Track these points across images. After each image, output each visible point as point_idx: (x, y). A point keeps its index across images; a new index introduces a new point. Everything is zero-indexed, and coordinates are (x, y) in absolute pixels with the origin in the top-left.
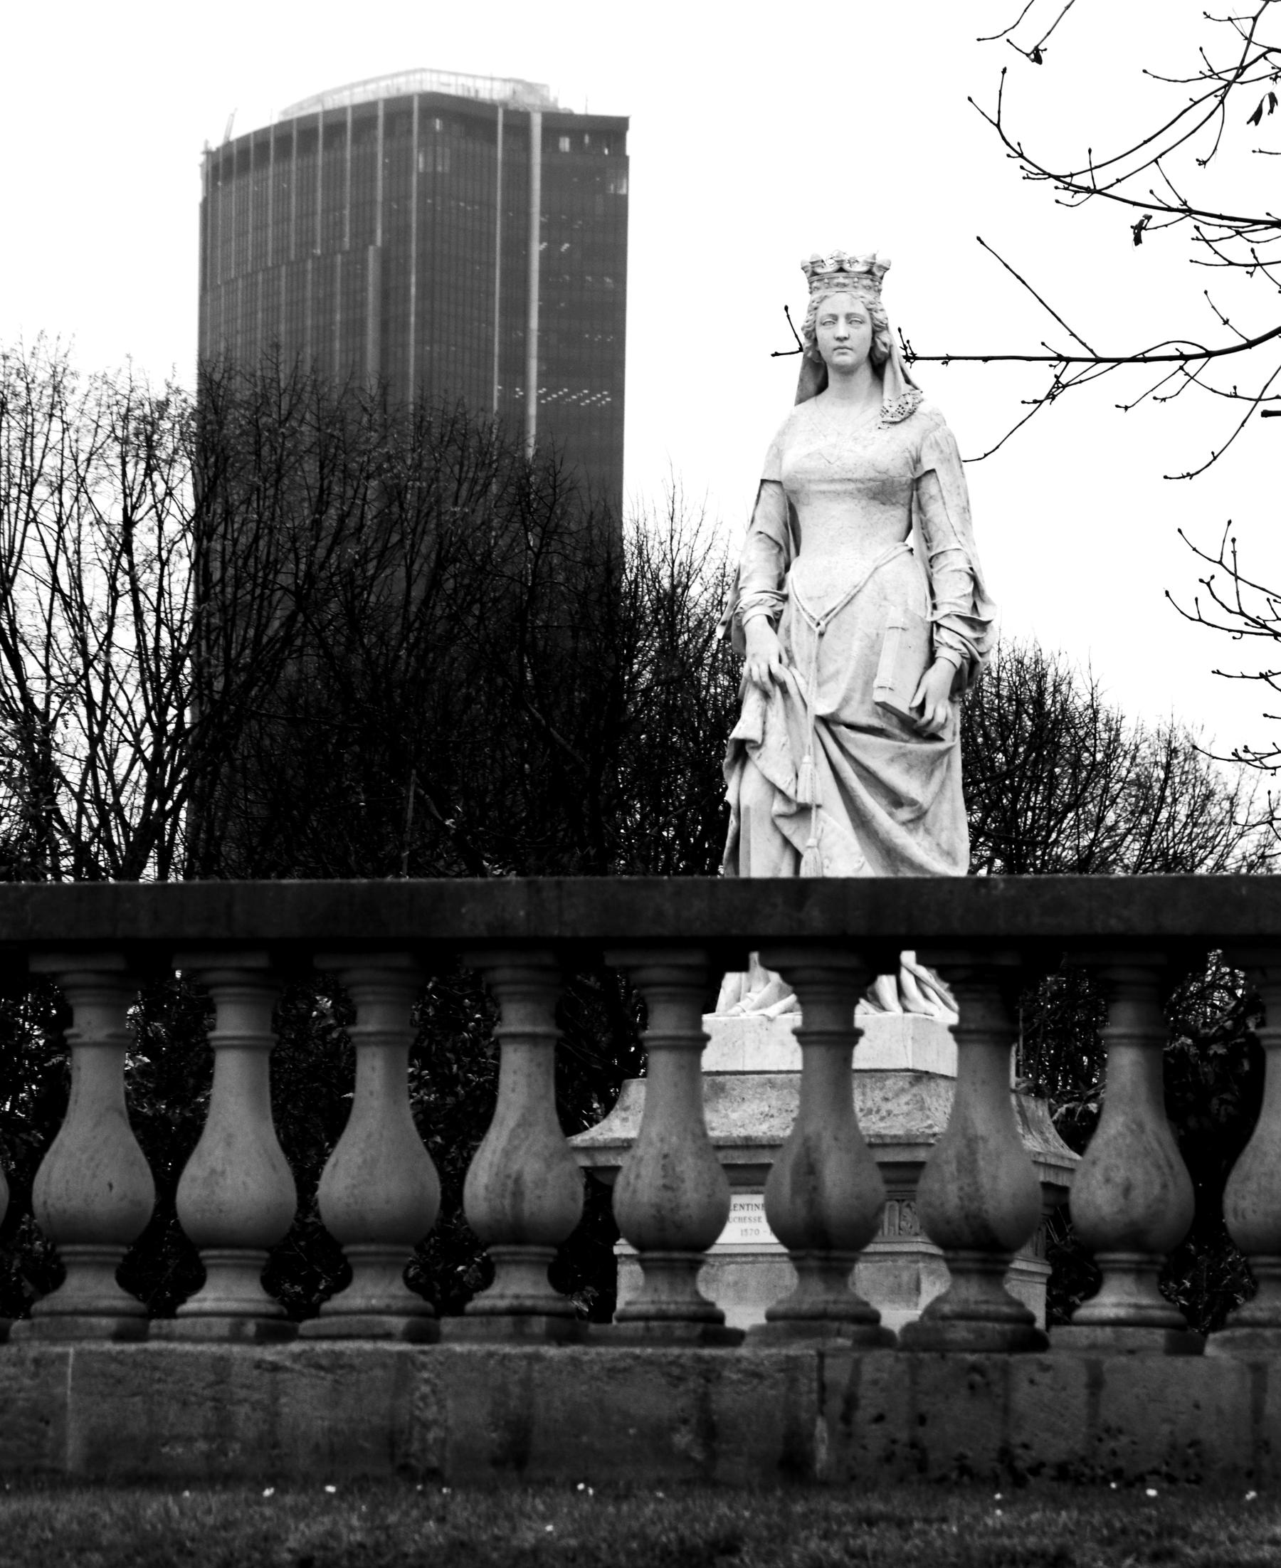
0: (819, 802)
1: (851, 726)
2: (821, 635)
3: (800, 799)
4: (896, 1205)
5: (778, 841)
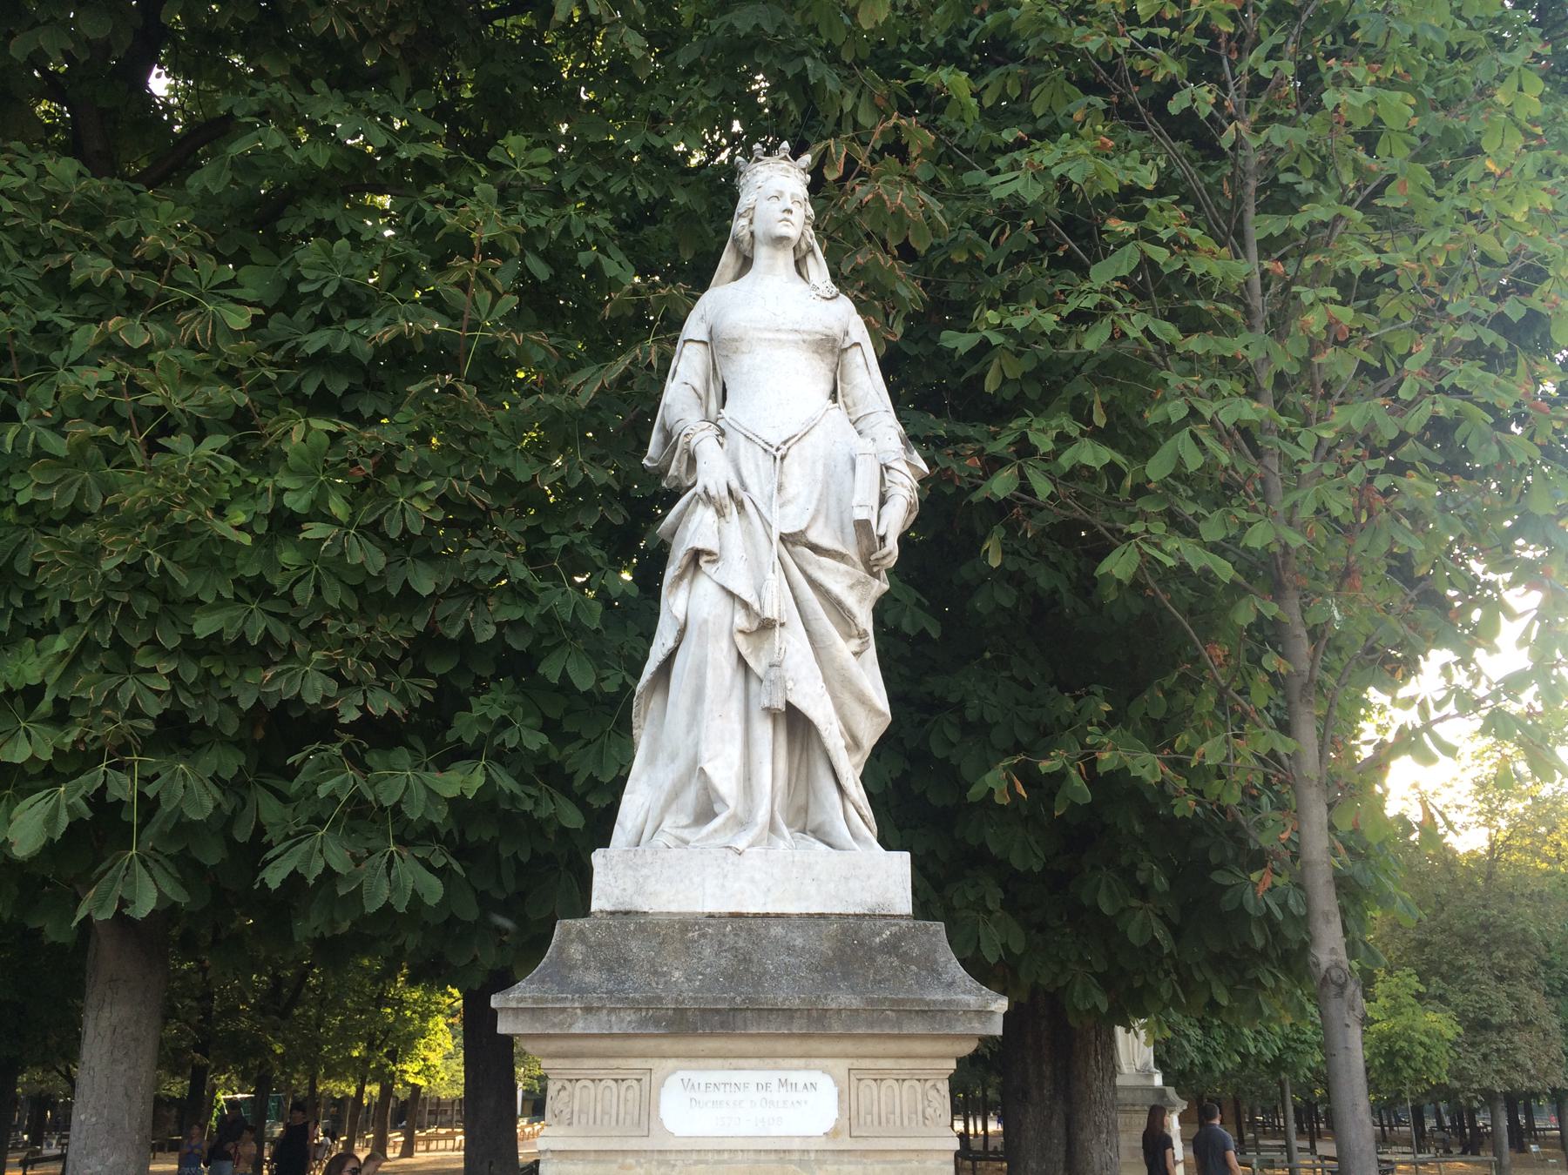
1: (815, 549)
2: (783, 458)
3: (768, 614)
4: (896, 1085)
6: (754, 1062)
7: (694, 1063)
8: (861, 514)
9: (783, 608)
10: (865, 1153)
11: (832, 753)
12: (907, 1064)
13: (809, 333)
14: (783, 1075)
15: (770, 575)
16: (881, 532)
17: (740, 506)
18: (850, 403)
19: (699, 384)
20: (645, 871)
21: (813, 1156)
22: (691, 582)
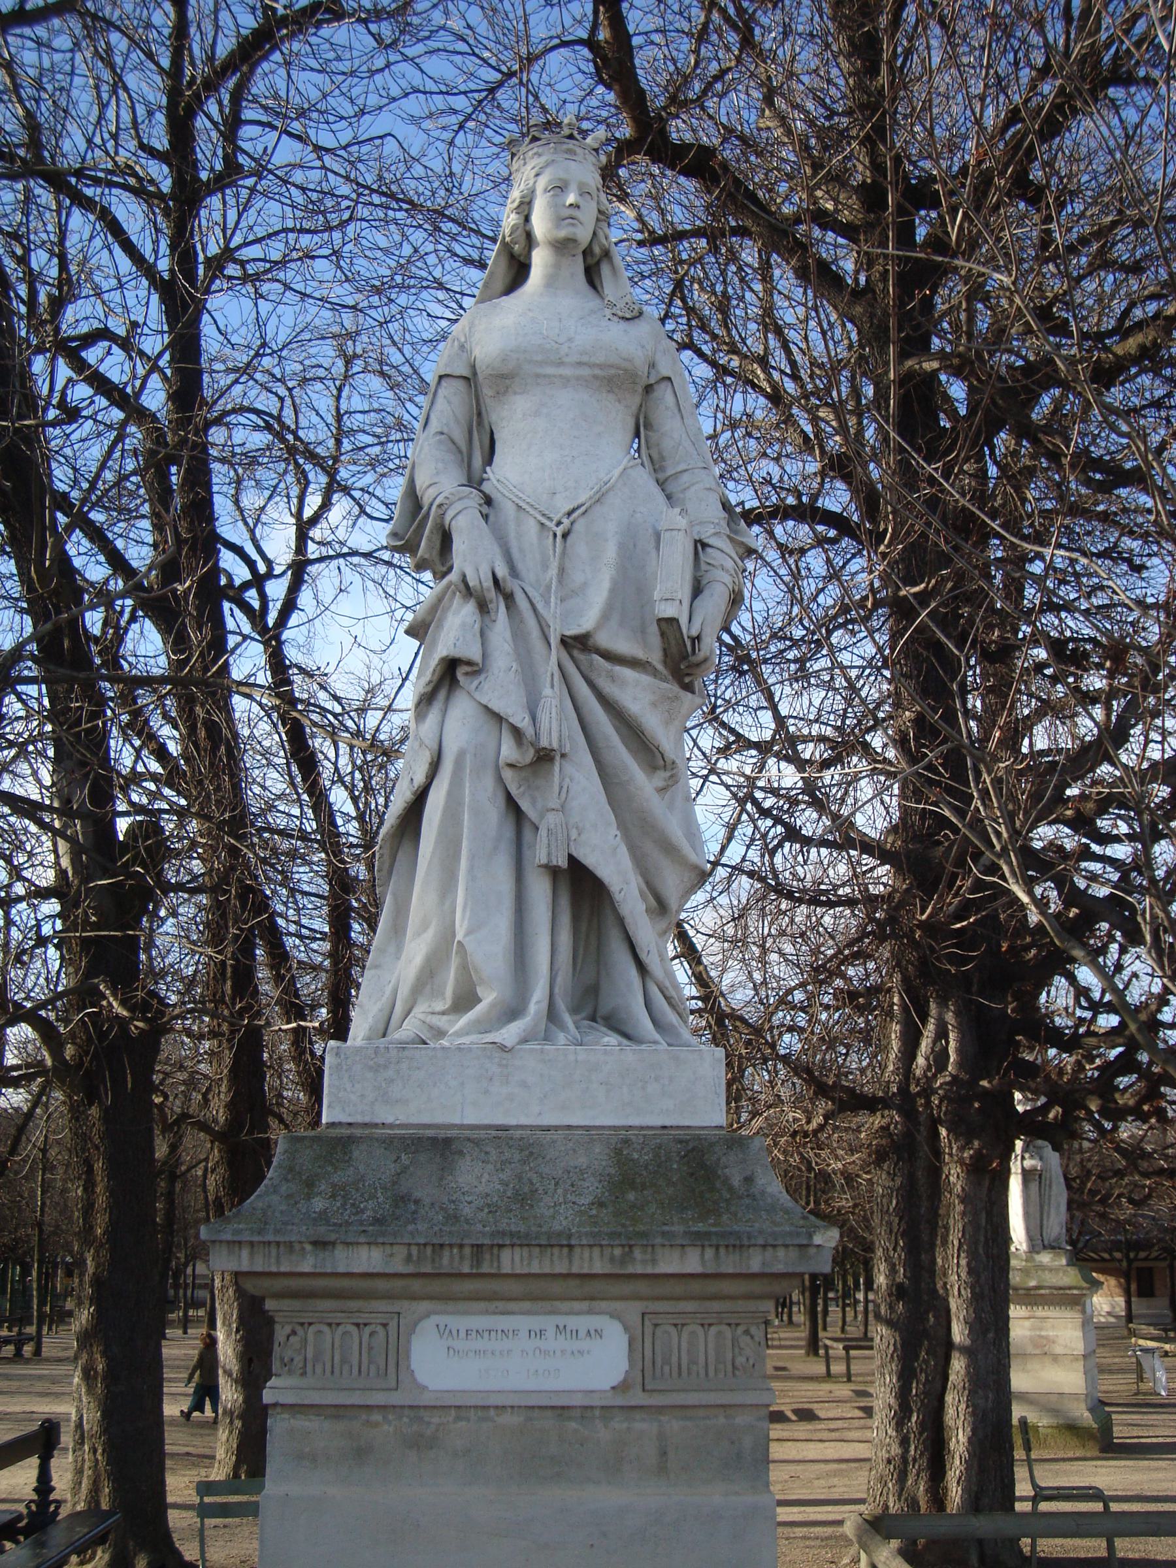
0: (567, 750)
2: (565, 536)
3: (544, 743)
5: (501, 801)
6: (527, 1305)
7: (451, 1306)
8: (669, 611)
9: (565, 733)
10: (661, 1409)
11: (629, 921)
12: (716, 1306)
13: (600, 366)
14: (561, 1320)
15: (547, 691)
16: (694, 633)
17: (509, 598)
18: (655, 456)
19: (459, 436)
20: (390, 1073)
21: (597, 1413)
22: (448, 699)
